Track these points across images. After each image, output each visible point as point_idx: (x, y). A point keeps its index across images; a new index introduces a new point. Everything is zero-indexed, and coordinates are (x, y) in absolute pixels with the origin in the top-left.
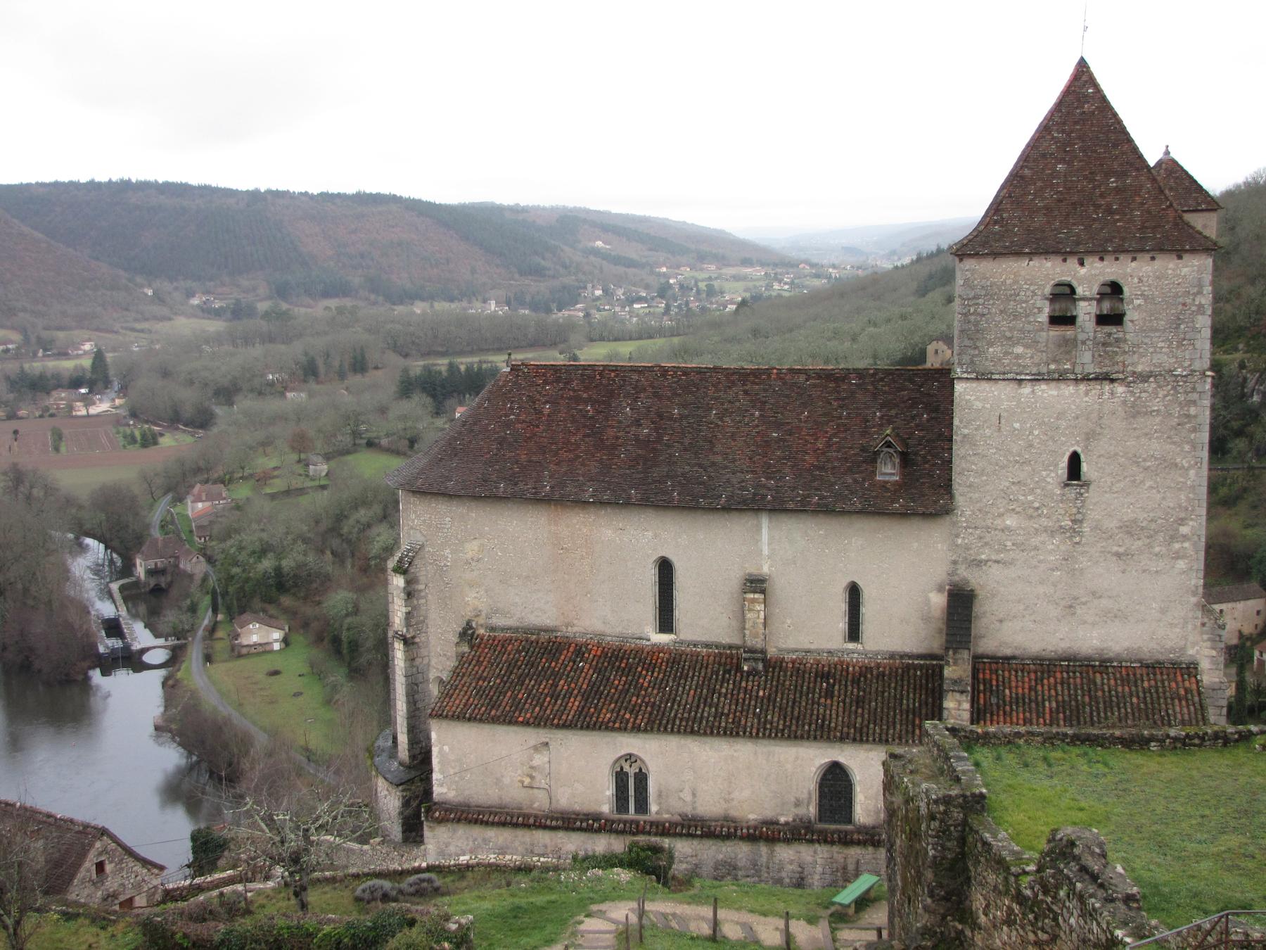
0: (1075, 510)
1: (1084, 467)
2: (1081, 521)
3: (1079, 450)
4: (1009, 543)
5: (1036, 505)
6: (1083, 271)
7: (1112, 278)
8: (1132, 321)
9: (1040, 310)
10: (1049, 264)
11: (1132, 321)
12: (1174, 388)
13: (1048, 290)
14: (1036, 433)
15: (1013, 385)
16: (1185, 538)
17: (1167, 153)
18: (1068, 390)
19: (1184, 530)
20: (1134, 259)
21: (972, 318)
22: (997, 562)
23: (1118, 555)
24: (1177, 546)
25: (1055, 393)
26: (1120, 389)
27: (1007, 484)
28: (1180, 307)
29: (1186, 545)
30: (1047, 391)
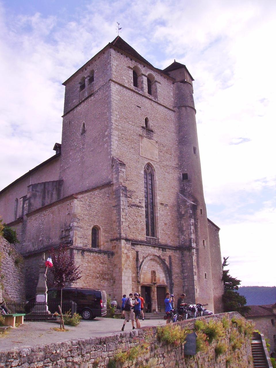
0: (83, 141)
2: (84, 144)
3: (84, 121)
4: (70, 160)
5: (76, 144)
6: (86, 71)
10: (80, 74)
12: (103, 89)
14: (76, 122)
16: (107, 136)
17: (175, 61)
19: (106, 133)
20: (95, 60)
22: (68, 168)
23: (92, 151)
24: (105, 140)
25: (80, 108)
26: (92, 98)
27: (71, 142)
29: (107, 138)
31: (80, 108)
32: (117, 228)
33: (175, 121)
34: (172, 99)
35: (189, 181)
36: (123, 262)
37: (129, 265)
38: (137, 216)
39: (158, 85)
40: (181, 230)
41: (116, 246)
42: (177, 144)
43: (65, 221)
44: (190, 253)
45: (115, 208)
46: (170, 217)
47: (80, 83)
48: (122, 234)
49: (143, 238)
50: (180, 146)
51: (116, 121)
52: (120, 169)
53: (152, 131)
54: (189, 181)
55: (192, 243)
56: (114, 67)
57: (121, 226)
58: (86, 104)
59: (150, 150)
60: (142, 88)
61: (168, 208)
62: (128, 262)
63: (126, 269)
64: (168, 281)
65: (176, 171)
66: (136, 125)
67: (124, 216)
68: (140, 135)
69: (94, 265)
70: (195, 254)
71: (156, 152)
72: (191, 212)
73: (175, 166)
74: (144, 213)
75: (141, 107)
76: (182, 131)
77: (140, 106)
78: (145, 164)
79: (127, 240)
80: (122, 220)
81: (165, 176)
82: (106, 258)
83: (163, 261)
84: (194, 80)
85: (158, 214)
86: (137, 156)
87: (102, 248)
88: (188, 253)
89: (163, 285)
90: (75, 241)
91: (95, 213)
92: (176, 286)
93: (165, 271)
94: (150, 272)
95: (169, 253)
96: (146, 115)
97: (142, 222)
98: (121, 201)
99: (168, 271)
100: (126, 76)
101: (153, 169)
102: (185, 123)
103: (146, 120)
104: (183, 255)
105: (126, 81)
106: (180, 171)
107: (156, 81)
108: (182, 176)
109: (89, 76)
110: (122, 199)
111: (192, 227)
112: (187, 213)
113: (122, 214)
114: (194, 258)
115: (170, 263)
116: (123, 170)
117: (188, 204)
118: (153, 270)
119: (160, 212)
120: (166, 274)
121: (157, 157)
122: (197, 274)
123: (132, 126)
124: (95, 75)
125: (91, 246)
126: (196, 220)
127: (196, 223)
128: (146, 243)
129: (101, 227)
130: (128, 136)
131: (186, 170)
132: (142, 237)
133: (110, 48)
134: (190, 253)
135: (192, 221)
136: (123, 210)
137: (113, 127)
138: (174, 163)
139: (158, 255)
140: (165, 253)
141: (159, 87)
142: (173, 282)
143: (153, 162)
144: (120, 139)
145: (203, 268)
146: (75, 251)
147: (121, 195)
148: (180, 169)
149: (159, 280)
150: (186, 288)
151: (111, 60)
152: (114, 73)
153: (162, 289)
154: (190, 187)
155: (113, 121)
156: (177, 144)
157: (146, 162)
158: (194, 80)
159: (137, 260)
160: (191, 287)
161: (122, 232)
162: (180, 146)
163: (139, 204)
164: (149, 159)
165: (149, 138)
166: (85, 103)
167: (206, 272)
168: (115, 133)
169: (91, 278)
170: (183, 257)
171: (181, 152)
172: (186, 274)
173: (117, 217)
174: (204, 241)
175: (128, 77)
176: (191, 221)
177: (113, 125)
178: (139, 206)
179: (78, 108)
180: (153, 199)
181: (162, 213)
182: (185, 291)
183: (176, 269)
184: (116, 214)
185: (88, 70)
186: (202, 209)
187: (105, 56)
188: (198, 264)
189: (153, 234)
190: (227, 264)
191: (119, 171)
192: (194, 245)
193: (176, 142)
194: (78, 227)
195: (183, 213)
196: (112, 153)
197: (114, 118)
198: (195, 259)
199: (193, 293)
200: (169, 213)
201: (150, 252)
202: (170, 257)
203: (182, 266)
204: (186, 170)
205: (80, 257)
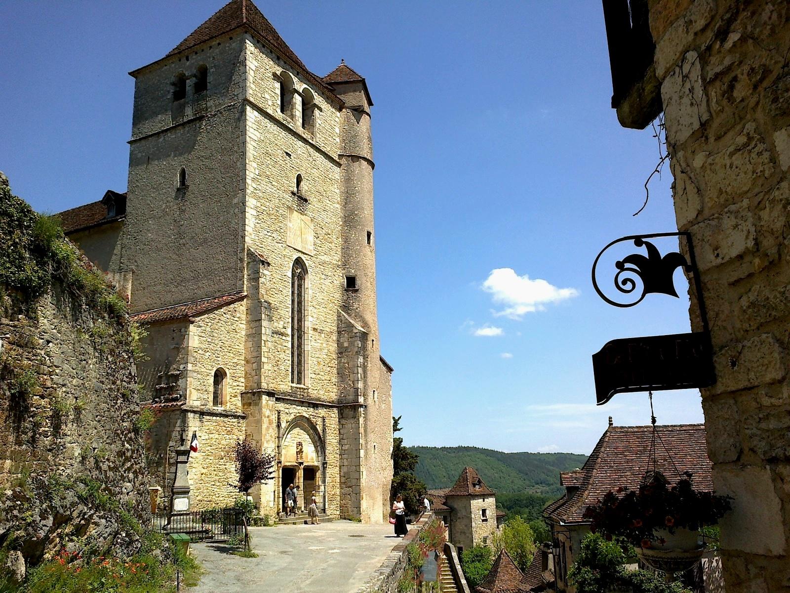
1: (186, 178)
6: (188, 63)
7: (201, 63)
8: (209, 83)
9: (169, 92)
10: (173, 65)
11: (209, 83)
13: (173, 79)
15: (154, 138)
18: (180, 131)
19: (235, 201)
20: (211, 47)
21: (139, 107)
25: (174, 136)
28: (232, 66)
30: (171, 136)
31: (174, 136)
32: (253, 373)
33: (339, 181)
34: (338, 140)
35: (357, 290)
36: (264, 431)
37: (271, 436)
38: (279, 350)
39: (317, 112)
40: (341, 374)
41: (251, 403)
42: (341, 223)
43: (167, 359)
44: (354, 412)
45: (250, 339)
46: (326, 351)
47: (173, 84)
48: (262, 384)
49: (287, 387)
50: (346, 228)
51: (253, 179)
52: (261, 271)
53: (306, 200)
54: (357, 290)
55: (359, 397)
56: (252, 73)
57: (262, 370)
58: (188, 132)
59: (301, 233)
60: (292, 117)
61: (323, 335)
62: (271, 430)
63: (267, 442)
64: (320, 458)
65: (338, 271)
66: (283, 188)
67: (266, 353)
68: (289, 208)
69: (217, 436)
70: (363, 415)
71: (310, 238)
72: (360, 346)
73: (335, 262)
74: (290, 345)
75: (292, 154)
76: (350, 201)
77: (290, 153)
78: (294, 260)
79: (270, 394)
80: (264, 360)
81: (322, 281)
82: (234, 424)
83: (314, 428)
84: (373, 105)
85: (310, 347)
86: (282, 245)
87: (228, 407)
88: (352, 412)
89: (313, 466)
90: (190, 395)
91: (219, 346)
92: (330, 466)
93: (314, 442)
94: (295, 445)
95: (322, 412)
96: (298, 169)
97: (286, 361)
98: (263, 328)
99: (320, 443)
100: (270, 92)
101: (304, 267)
102: (357, 189)
103: (299, 179)
104: (342, 415)
105: (270, 103)
106: (343, 272)
107: (315, 106)
108: (346, 281)
109: (195, 76)
110: (265, 323)
111: (360, 370)
112: (354, 345)
113: (264, 349)
114: (361, 420)
115: (324, 430)
116: (266, 272)
117: (356, 331)
118: (299, 440)
119: (313, 343)
120: (316, 447)
121: (312, 248)
122: (364, 445)
123: (278, 191)
124: (210, 79)
125: (212, 404)
126: (365, 357)
127: (366, 363)
128: (291, 396)
129: (227, 371)
130: (271, 209)
131: (353, 271)
132: (285, 386)
133: (246, 33)
134: (354, 412)
135: (361, 360)
136: (265, 344)
137: (248, 191)
138: (336, 258)
139: (307, 416)
140: (316, 411)
141: (319, 116)
142: (327, 459)
143: (305, 256)
144: (259, 213)
145: (371, 436)
146: (191, 415)
147: (263, 316)
148: (344, 269)
149: (307, 457)
150: (345, 469)
151: (247, 57)
152: (252, 86)
153: (310, 473)
154: (359, 301)
155: (249, 181)
156: (341, 223)
157: (295, 257)
158: (373, 105)
159: (279, 426)
160: (354, 467)
161: (263, 381)
162: (346, 228)
163: (283, 330)
164: (299, 251)
165: (301, 214)
166: (187, 129)
167: (375, 444)
168: (251, 202)
169: (212, 458)
170: (342, 418)
171: (346, 240)
172: (346, 447)
173: (255, 354)
174: (374, 391)
175: (273, 94)
176: (359, 360)
177: (250, 188)
178: (282, 334)
179: (169, 134)
180: (300, 320)
181: (315, 344)
182: (342, 474)
183: (332, 440)
184: (252, 349)
185: (192, 62)
186: (374, 339)
187: (234, 45)
188: (365, 431)
189: (299, 382)
190: (398, 427)
191: (261, 274)
192: (361, 400)
193: (340, 219)
194: (195, 372)
195: (346, 344)
196: (247, 239)
197: (250, 174)
198: (362, 422)
199: (357, 479)
200: (324, 345)
201: (296, 411)
202: (324, 419)
203: (339, 432)
204: (353, 271)
205: (198, 423)
